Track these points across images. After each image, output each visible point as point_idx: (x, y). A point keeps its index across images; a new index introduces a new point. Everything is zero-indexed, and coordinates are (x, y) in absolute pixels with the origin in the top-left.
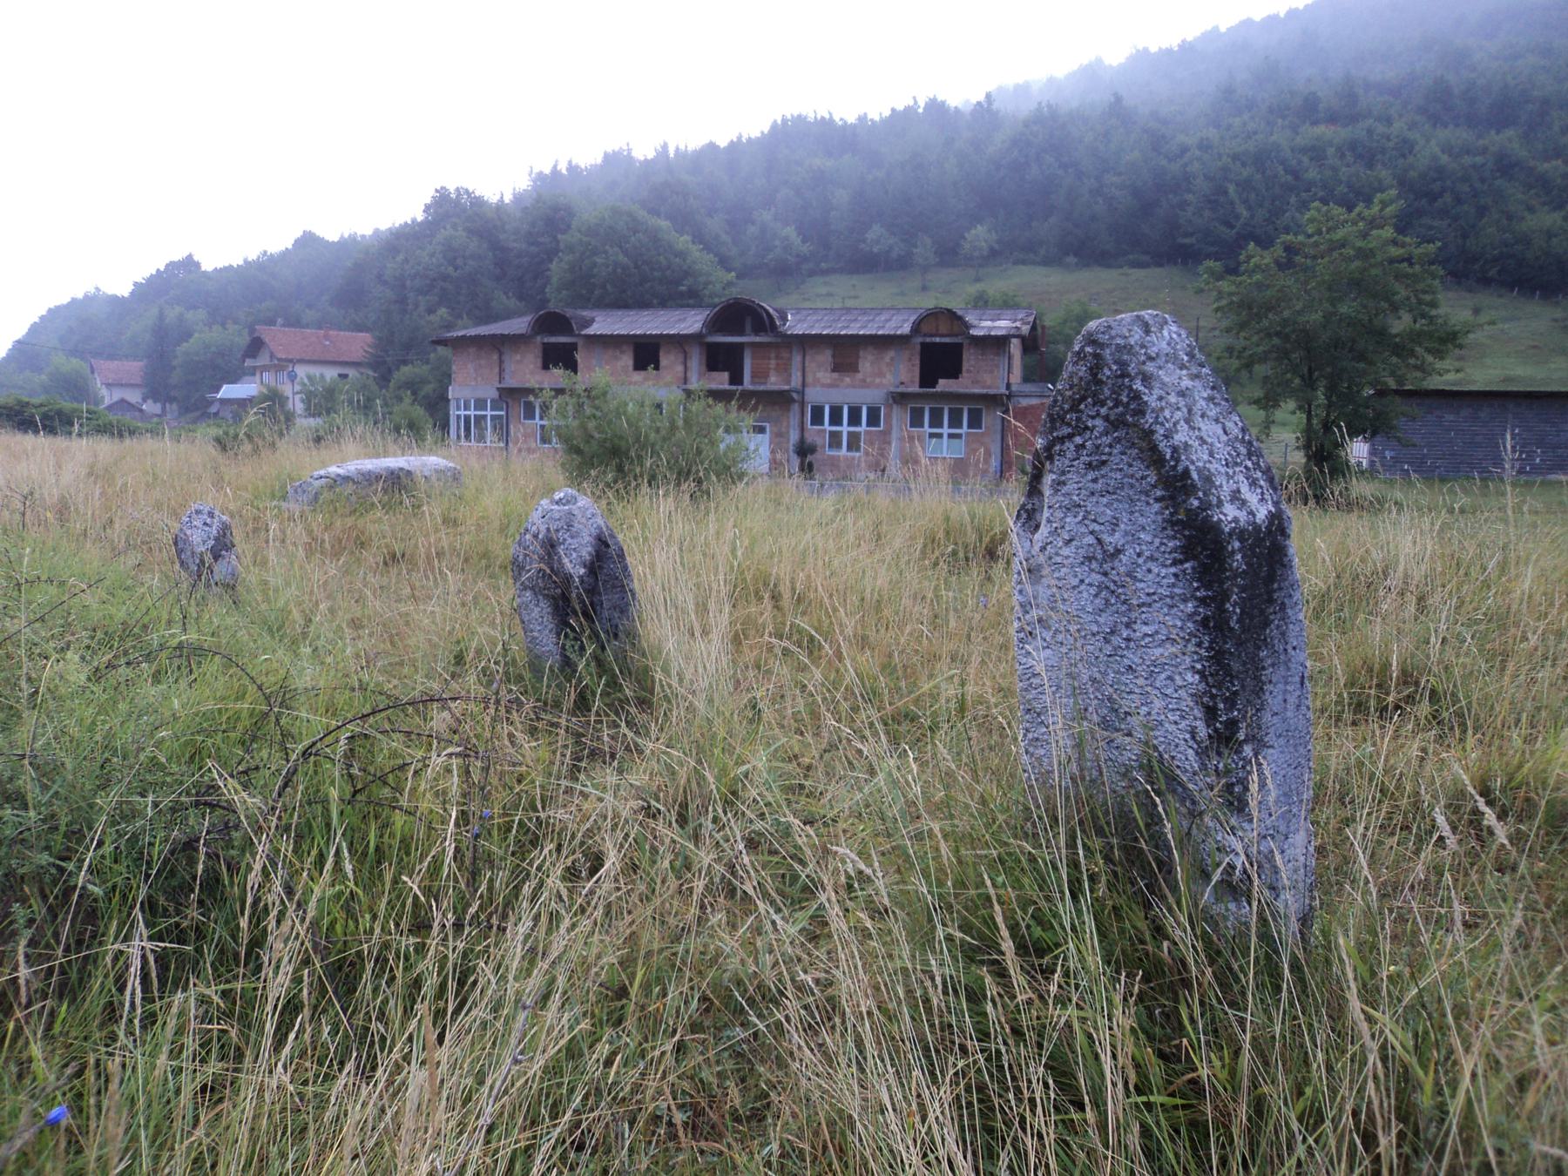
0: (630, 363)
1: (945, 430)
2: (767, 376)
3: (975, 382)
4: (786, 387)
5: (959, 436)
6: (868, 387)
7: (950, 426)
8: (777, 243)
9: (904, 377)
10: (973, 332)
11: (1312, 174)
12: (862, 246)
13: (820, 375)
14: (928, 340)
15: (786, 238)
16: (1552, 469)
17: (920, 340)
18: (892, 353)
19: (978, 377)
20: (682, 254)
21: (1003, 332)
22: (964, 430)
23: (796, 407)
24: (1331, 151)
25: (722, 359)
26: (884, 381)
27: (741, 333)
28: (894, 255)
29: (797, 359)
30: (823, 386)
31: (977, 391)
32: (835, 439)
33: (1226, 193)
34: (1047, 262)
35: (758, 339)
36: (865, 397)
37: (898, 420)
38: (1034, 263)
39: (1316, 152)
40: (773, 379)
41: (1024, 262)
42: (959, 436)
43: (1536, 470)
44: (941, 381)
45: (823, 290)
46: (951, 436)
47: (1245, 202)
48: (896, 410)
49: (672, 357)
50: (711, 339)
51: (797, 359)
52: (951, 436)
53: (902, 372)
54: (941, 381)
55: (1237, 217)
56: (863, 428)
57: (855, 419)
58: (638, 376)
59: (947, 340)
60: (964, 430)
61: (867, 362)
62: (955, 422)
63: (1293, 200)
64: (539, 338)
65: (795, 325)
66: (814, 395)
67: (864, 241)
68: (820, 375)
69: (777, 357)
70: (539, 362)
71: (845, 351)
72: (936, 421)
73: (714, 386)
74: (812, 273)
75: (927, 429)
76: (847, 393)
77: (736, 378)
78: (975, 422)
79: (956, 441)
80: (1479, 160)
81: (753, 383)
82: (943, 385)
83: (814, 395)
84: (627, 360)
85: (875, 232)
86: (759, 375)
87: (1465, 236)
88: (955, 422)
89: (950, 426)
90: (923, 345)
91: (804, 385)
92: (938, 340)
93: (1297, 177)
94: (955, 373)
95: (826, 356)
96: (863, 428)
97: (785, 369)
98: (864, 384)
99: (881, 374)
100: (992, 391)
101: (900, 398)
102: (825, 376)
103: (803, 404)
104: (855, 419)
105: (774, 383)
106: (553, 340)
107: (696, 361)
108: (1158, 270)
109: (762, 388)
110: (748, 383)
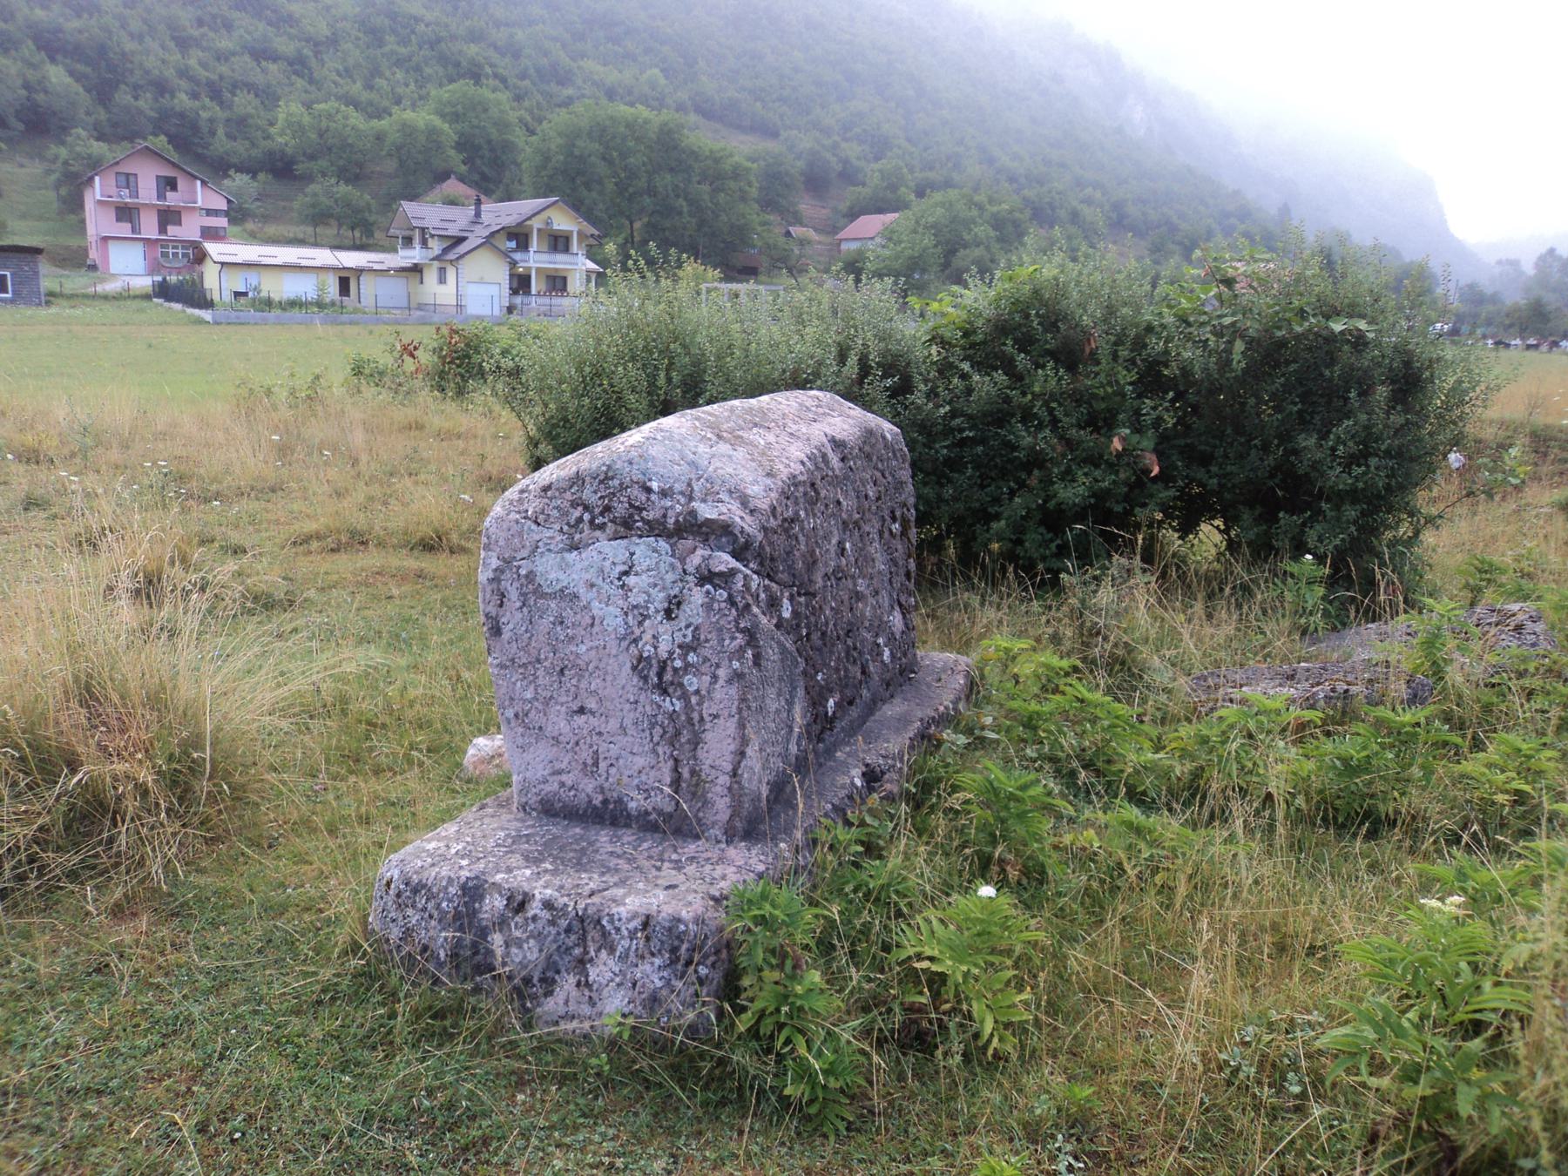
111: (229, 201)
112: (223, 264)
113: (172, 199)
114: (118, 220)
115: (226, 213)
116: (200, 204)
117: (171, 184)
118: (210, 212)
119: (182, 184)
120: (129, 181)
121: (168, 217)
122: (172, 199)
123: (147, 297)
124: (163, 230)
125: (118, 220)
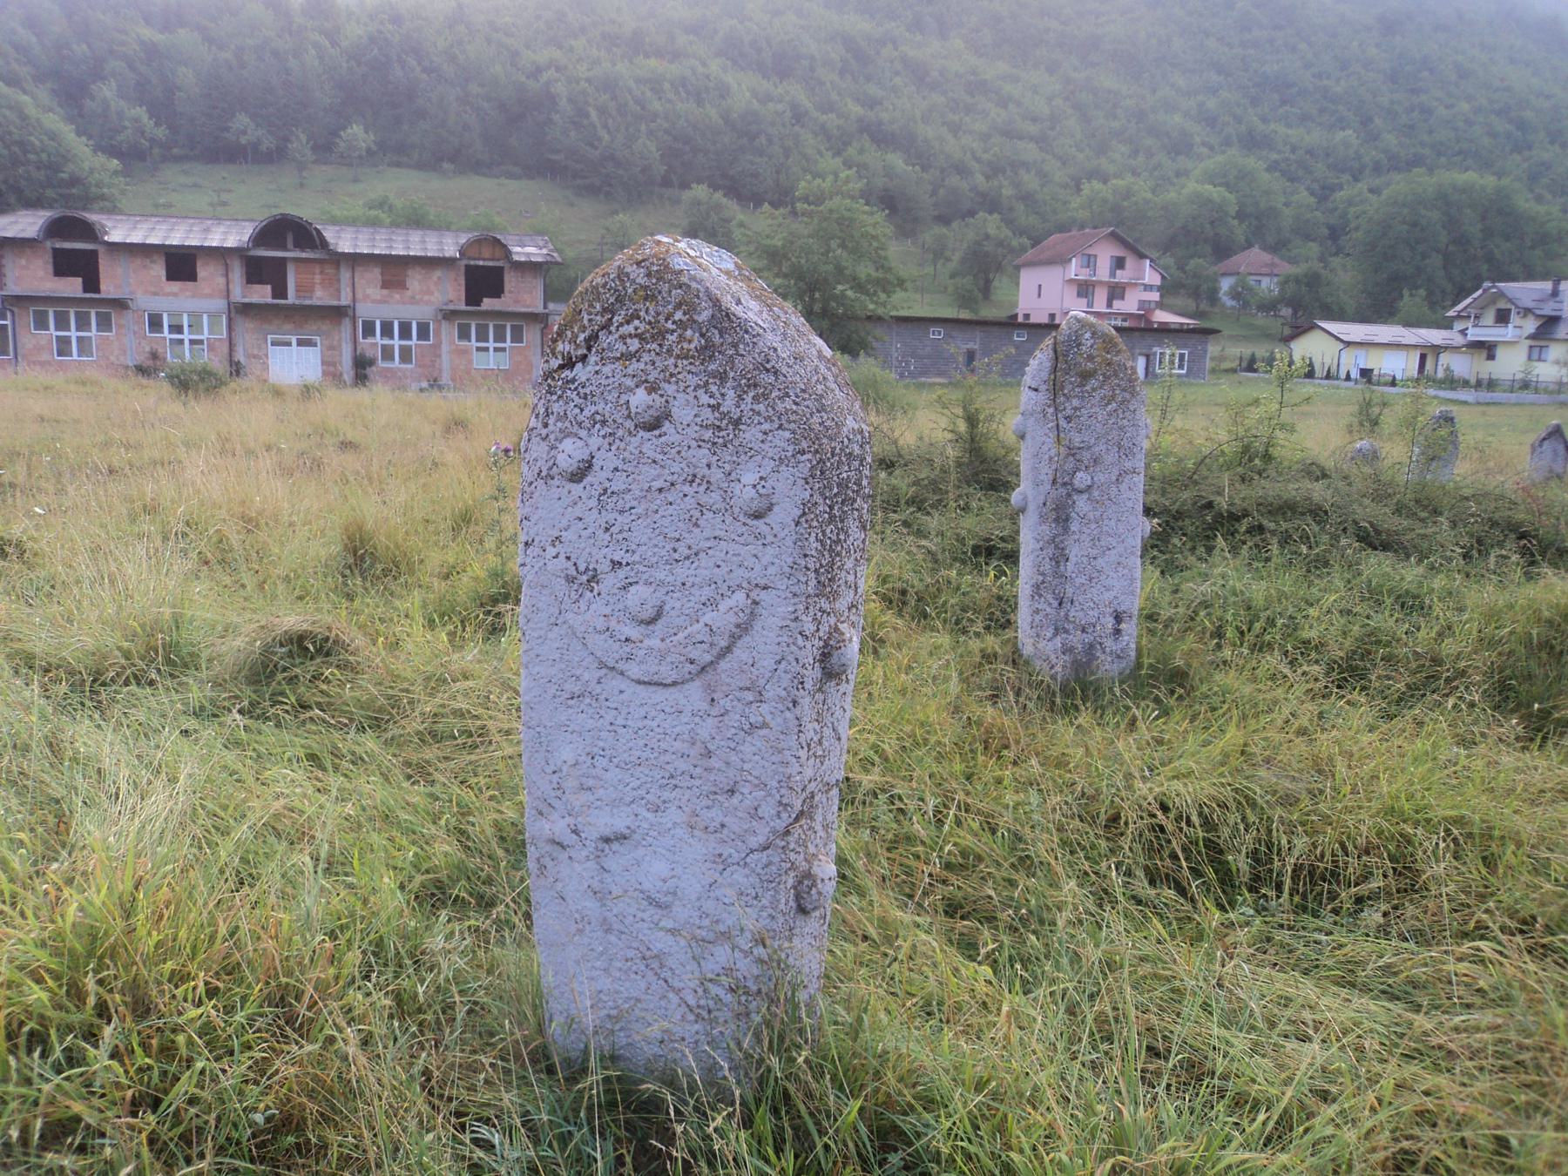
0: (163, 273)
1: (491, 344)
2: (312, 291)
3: (517, 302)
4: (335, 303)
6: (417, 303)
8: (127, 123)
9: (451, 296)
10: (516, 258)
11: (656, 106)
12: (226, 135)
13: (369, 291)
15: (137, 120)
16: (924, 373)
17: (465, 262)
18: (438, 273)
19: (523, 295)
20: (53, 136)
21: (540, 259)
22: (508, 344)
23: (347, 322)
24: (667, 86)
25: (258, 271)
27: (285, 248)
28: (263, 148)
29: (345, 275)
30: (373, 301)
31: (523, 310)
32: (387, 353)
33: (587, 116)
34: (421, 166)
35: (304, 255)
36: (416, 313)
37: (447, 335)
38: (409, 166)
39: (655, 84)
40: (319, 293)
41: (398, 165)
42: (503, 349)
43: (912, 375)
44: (486, 300)
45: (182, 179)
46: (496, 349)
47: (605, 126)
48: (444, 324)
49: (211, 268)
50: (252, 253)
51: (345, 275)
53: (449, 290)
54: (486, 300)
55: (600, 139)
56: (414, 342)
57: (405, 332)
58: (175, 286)
59: (491, 264)
60: (508, 344)
62: (500, 338)
63: (643, 127)
64: (48, 244)
65: (344, 241)
66: (364, 311)
67: (227, 129)
68: (369, 291)
70: (50, 268)
71: (394, 269)
72: (482, 336)
73: (255, 299)
74: (164, 159)
75: (474, 343)
76: (396, 308)
77: (280, 292)
78: (517, 338)
79: (499, 354)
80: (780, 107)
81: (298, 297)
82: (488, 304)
83: (364, 311)
84: (159, 270)
85: (242, 120)
87: (778, 172)
88: (500, 338)
91: (354, 300)
93: (643, 109)
94: (497, 292)
95: (375, 273)
96: (414, 342)
97: (333, 284)
99: (430, 293)
101: (450, 315)
102: (375, 292)
104: (405, 332)
105: (320, 297)
106: (67, 245)
107: (237, 274)
109: (308, 302)
110: (292, 298)
111: (1163, 277)
112: (1348, 344)
113: (1122, 276)
114: (1079, 295)
115: (1159, 289)
116: (1146, 281)
117: (1119, 263)
118: (1148, 288)
119: (1130, 262)
120: (1090, 262)
121: (1116, 292)
122: (1122, 276)
123: (1234, 371)
124: (1109, 305)
125: (1079, 295)
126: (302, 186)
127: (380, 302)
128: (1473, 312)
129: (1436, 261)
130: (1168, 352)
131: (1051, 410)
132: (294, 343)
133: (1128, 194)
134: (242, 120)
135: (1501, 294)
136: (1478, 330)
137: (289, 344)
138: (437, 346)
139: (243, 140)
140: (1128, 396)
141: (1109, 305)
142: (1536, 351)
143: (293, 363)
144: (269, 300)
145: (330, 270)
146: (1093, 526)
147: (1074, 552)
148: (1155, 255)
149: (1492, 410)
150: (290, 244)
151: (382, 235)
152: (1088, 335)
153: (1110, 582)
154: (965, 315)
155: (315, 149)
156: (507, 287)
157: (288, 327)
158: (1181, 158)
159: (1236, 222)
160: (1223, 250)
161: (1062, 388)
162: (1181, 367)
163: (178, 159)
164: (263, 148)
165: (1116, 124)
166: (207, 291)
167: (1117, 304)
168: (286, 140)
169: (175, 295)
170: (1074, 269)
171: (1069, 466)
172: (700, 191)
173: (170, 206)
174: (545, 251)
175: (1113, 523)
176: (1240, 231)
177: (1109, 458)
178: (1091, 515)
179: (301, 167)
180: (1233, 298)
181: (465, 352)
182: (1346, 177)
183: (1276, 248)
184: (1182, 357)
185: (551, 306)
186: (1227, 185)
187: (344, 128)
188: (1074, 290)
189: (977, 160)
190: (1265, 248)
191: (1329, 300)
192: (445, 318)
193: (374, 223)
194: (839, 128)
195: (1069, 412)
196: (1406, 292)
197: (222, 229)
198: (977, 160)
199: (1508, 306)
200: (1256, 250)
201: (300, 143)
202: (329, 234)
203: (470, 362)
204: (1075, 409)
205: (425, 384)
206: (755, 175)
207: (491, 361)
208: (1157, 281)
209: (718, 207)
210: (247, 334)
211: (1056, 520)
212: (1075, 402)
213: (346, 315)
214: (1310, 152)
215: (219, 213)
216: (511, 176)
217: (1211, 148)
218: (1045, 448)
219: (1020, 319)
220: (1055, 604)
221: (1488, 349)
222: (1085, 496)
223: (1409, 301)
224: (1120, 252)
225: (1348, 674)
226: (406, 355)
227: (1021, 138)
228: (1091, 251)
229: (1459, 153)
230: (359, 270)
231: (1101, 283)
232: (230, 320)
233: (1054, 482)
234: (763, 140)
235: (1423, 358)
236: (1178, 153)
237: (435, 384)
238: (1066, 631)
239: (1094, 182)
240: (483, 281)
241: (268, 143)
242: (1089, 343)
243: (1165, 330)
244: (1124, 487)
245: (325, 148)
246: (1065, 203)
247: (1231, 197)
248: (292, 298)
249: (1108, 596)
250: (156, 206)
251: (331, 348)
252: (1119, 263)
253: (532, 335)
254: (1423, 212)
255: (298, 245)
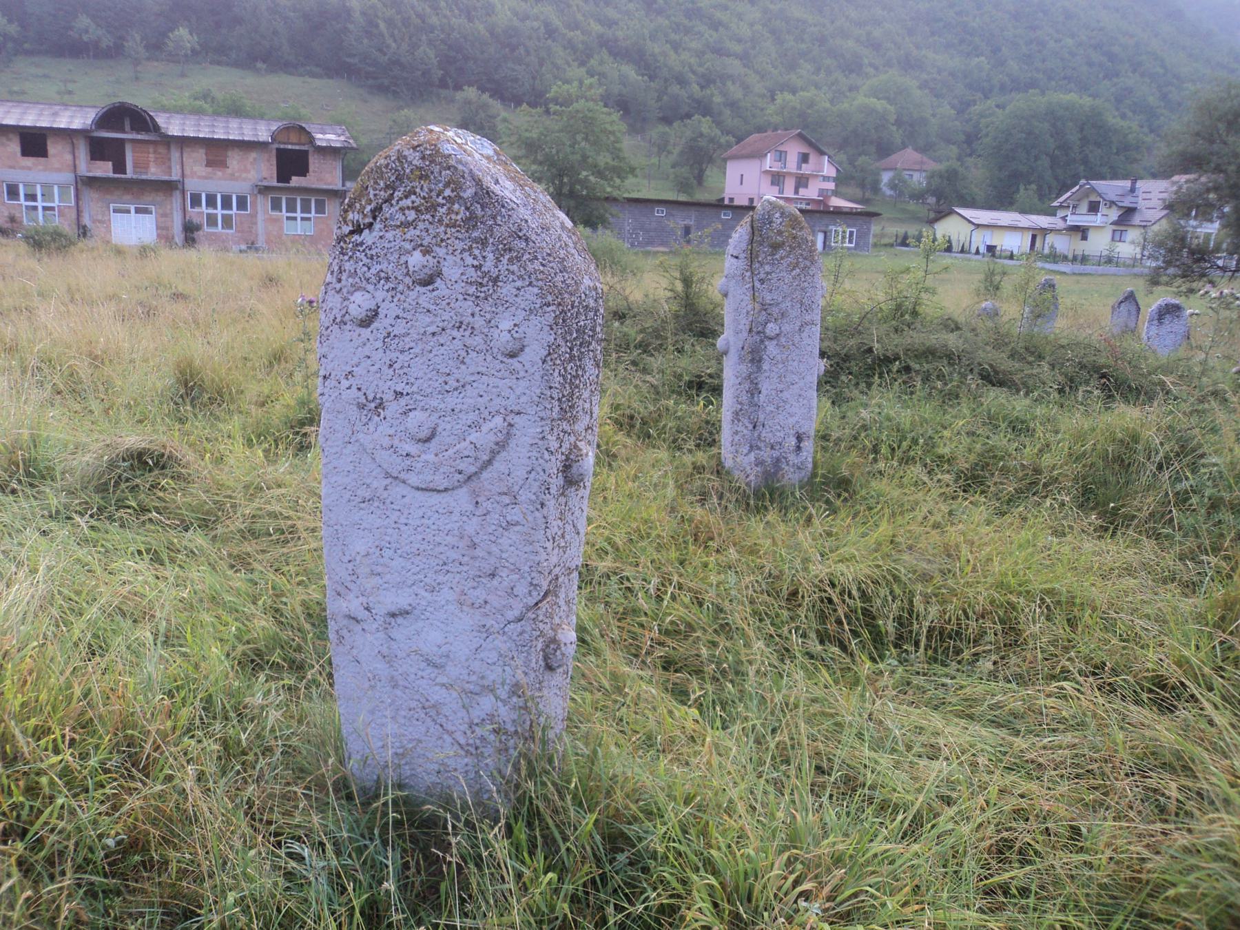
0: (18, 149)
1: (299, 215)
2: (147, 168)
4: (166, 178)
5: (309, 219)
6: (236, 179)
7: (302, 212)
9: (265, 174)
10: (319, 143)
11: (434, 20)
13: (196, 168)
14: (282, 146)
16: (650, 242)
17: (276, 146)
18: (253, 155)
19: (324, 175)
21: (338, 145)
23: (177, 194)
25: (100, 149)
26: (250, 176)
27: (123, 131)
28: (104, 45)
29: (175, 155)
30: (200, 177)
31: (325, 187)
32: (212, 220)
33: (377, 26)
34: (237, 64)
35: (139, 137)
36: (236, 188)
37: (263, 205)
40: (153, 170)
41: (219, 63)
42: (309, 219)
44: (294, 178)
46: (302, 219)
47: (392, 35)
49: (59, 147)
51: (175, 155)
52: (302, 219)
53: (263, 169)
54: (294, 178)
55: (388, 47)
57: (227, 204)
58: (29, 161)
59: (297, 147)
61: (234, 160)
62: (306, 209)
63: (424, 37)
65: (174, 126)
66: (192, 185)
67: (71, 28)
68: (196, 168)
69: (155, 152)
71: (217, 151)
72: (291, 208)
73: (99, 174)
76: (218, 183)
77: (120, 167)
78: (320, 208)
80: (536, 24)
81: (135, 172)
82: (296, 181)
84: (14, 147)
86: (140, 166)
87: (534, 78)
88: (306, 209)
89: (302, 212)
90: (278, 150)
91: (183, 175)
92: (290, 147)
93: (423, 22)
94: (303, 172)
95: (200, 154)
97: (165, 162)
98: (232, 177)
99: (247, 171)
100: (335, 188)
101: (264, 190)
103: (183, 192)
104: (227, 204)
105: (154, 173)
108: (331, 81)
109: (144, 177)
110: (130, 173)
112: (978, 226)
113: (806, 169)
114: (773, 183)
115: (835, 179)
116: (825, 173)
117: (804, 158)
118: (826, 179)
120: (781, 156)
121: (802, 181)
122: (806, 169)
123: (892, 245)
124: (796, 192)
125: (773, 183)
126: (137, 78)
127: (205, 178)
128: (1071, 203)
129: (1045, 162)
130: (840, 229)
131: (748, 274)
132: (133, 211)
133: (812, 104)
134: (84, 21)
135: (1093, 190)
136: (1074, 217)
137: (128, 212)
138: (254, 216)
139: (85, 38)
140: (808, 263)
141: (796, 192)
142: (1118, 234)
143: (132, 227)
144: (111, 175)
145: (162, 150)
146: (780, 366)
147: (765, 387)
148: (831, 153)
149: (1084, 279)
150: (127, 127)
151: (206, 121)
152: (777, 215)
153: (793, 410)
154: (683, 198)
155: (147, 47)
156: (311, 168)
157: (128, 197)
158: (854, 75)
159: (894, 128)
160: (884, 150)
161: (757, 256)
162: (850, 242)
163: (29, 53)
164: (104, 45)
165: (803, 46)
166: (57, 165)
167: (802, 191)
168: (122, 38)
169: (29, 169)
170: (769, 162)
171: (762, 318)
172: (471, 92)
173: (23, 93)
174: (342, 138)
175: (795, 364)
176: (897, 136)
177: (794, 313)
178: (779, 357)
179: (137, 62)
180: (892, 189)
181: (276, 221)
182: (979, 95)
183: (925, 149)
184: (851, 233)
185: (348, 184)
186: (888, 99)
187: (172, 30)
188: (769, 179)
189: (694, 72)
190: (916, 150)
191: (965, 191)
192: (260, 192)
193: (198, 112)
194: (583, 43)
195: (762, 276)
196: (1022, 187)
197: (68, 113)
198: (694, 72)
199: (1098, 199)
200: (909, 150)
201: (134, 42)
202: (161, 120)
203: (281, 228)
204: (768, 273)
205: (243, 247)
206: (516, 80)
207: (299, 228)
208: (833, 174)
209: (484, 107)
210: (93, 204)
211: (752, 361)
212: (768, 268)
213: (177, 188)
214: (952, 74)
215: (66, 100)
216: (313, 75)
217: (876, 69)
218: (743, 304)
219: (726, 202)
220: (751, 427)
221: (1081, 232)
222: (775, 342)
223: (1025, 193)
224: (805, 150)
225: (973, 481)
226: (227, 222)
227: (728, 55)
228: (781, 148)
229: (1065, 78)
230: (187, 150)
231: (790, 174)
232: (77, 190)
233: (751, 330)
234: (522, 50)
235: (1034, 237)
236: (851, 71)
237: (252, 246)
238: (759, 449)
239: (786, 93)
240: (291, 162)
241: (107, 41)
242: (779, 221)
243: (839, 213)
244: (805, 335)
245: (156, 46)
246: (762, 110)
247: (892, 108)
248: (130, 173)
249: (791, 421)
250: (11, 93)
251: (164, 215)
252: (804, 158)
253: (333, 208)
254: (1036, 124)
255: (134, 128)
